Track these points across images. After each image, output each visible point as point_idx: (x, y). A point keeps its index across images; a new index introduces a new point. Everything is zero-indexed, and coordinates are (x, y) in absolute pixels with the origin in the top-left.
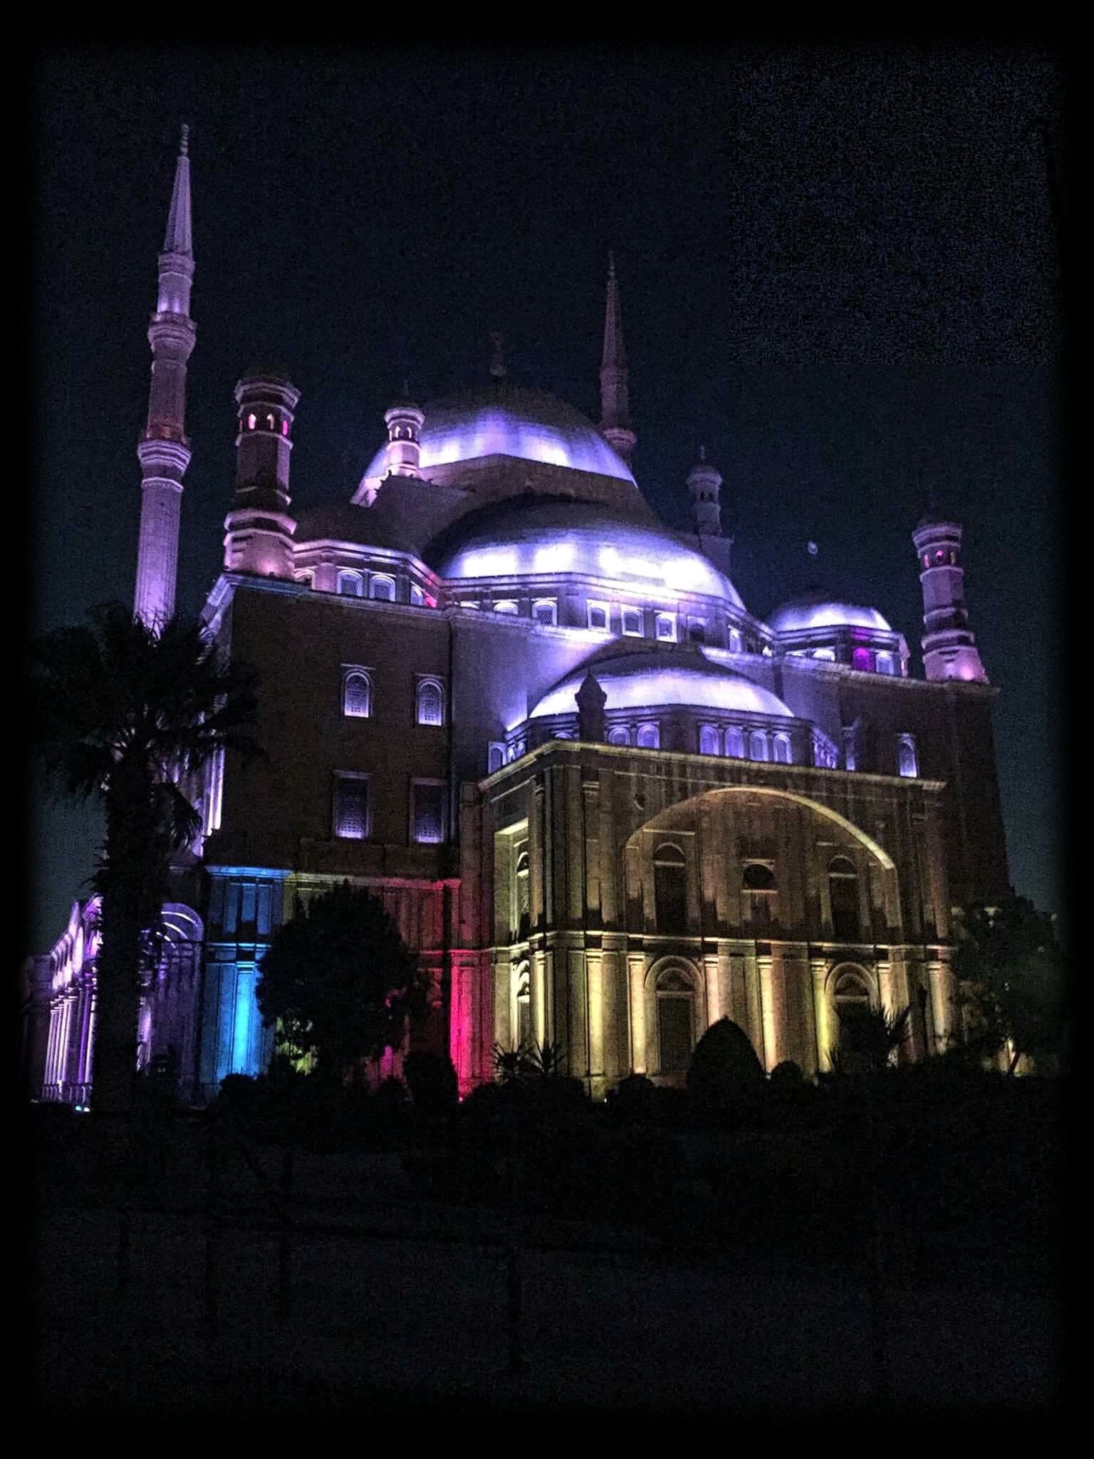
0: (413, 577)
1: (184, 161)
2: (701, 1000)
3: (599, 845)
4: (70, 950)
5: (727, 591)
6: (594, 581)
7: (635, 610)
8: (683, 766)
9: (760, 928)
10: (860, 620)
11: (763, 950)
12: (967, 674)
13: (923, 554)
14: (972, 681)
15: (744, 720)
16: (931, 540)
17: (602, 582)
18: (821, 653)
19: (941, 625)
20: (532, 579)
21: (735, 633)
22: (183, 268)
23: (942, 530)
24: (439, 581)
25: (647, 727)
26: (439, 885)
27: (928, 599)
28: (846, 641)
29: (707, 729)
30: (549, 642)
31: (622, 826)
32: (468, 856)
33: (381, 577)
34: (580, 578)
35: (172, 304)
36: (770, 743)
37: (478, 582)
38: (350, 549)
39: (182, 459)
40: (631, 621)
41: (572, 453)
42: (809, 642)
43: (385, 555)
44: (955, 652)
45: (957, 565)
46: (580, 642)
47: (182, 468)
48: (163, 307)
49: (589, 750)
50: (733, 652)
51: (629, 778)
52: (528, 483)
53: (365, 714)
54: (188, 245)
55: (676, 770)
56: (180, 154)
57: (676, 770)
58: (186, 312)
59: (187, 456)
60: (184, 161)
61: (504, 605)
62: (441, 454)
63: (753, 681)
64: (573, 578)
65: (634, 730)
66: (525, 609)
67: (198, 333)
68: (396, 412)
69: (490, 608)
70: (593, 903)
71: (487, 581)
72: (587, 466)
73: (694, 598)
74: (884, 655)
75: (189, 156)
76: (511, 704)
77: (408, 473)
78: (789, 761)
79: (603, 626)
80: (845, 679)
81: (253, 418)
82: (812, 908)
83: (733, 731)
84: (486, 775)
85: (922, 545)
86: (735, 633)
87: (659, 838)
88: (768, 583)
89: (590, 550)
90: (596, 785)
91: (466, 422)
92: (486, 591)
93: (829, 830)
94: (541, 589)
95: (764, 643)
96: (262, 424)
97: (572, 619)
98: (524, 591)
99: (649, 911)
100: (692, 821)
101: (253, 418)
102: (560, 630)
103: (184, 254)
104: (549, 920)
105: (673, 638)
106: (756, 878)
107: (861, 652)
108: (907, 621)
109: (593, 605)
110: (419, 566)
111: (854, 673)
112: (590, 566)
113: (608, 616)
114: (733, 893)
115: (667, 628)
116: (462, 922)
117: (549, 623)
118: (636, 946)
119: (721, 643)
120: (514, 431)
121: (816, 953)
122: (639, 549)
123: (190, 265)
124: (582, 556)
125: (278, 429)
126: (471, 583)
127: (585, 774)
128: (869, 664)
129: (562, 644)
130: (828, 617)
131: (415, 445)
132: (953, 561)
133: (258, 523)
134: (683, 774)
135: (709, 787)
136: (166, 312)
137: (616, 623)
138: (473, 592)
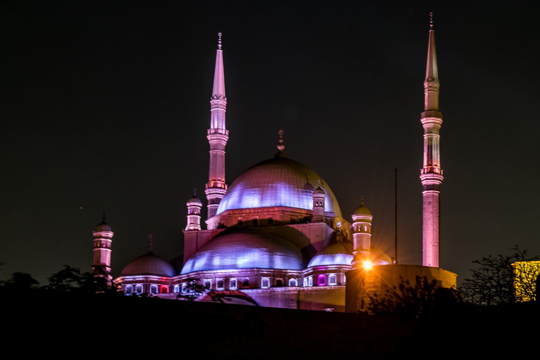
1: (220, 53)
6: (206, 272)
7: (221, 279)
33: (138, 285)
35: (218, 123)
38: (129, 278)
40: (220, 284)
43: (140, 278)
52: (240, 218)
56: (218, 48)
60: (220, 53)
64: (199, 272)
122: (228, 255)
123: (223, 102)
128: (324, 281)
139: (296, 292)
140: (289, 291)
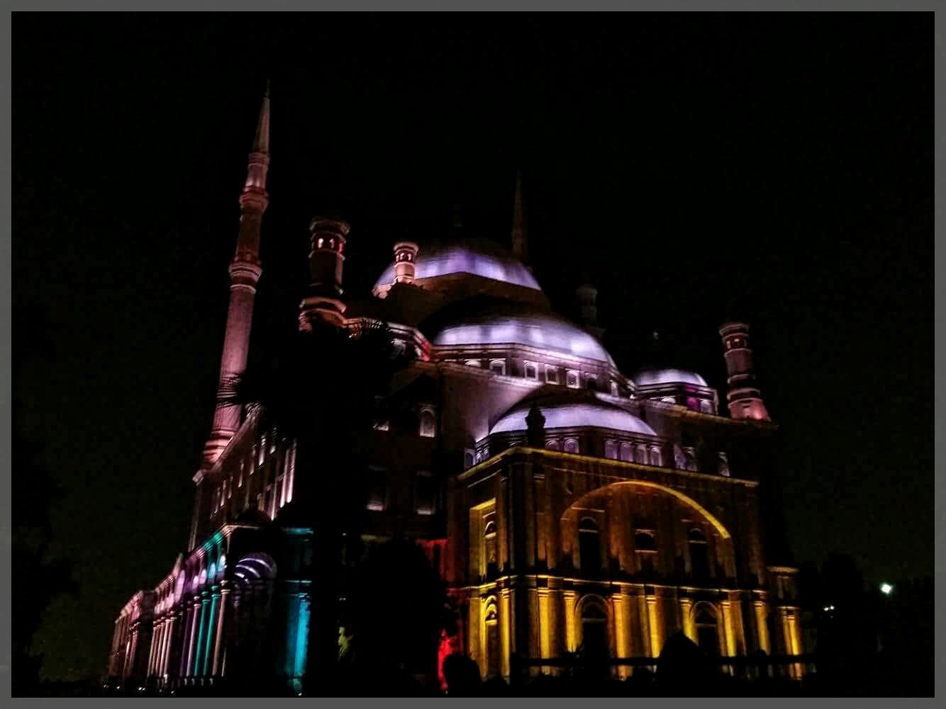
0: (417, 343)
1: (267, 103)
2: (610, 626)
3: (544, 516)
4: (172, 587)
5: (608, 359)
6: (528, 349)
8: (596, 465)
9: (645, 575)
10: (690, 380)
11: (650, 591)
12: (758, 415)
13: (727, 340)
14: (762, 421)
15: (632, 437)
16: (730, 332)
17: (533, 350)
18: (666, 399)
19: (739, 384)
20: (490, 347)
21: (614, 385)
22: (263, 162)
23: (738, 326)
24: (431, 347)
25: (571, 441)
26: (432, 543)
27: (730, 369)
28: (681, 392)
29: (609, 442)
30: (501, 386)
31: (559, 505)
32: (451, 526)
34: (520, 347)
36: (649, 452)
37: (455, 348)
39: (256, 273)
40: (551, 375)
41: (507, 273)
42: (659, 392)
44: (749, 401)
45: (747, 347)
46: (525, 385)
47: (256, 278)
48: (250, 183)
49: (539, 454)
50: (614, 396)
51: (563, 472)
53: (387, 429)
54: (267, 149)
55: (591, 468)
56: (265, 96)
57: (591, 468)
58: (264, 187)
59: (259, 271)
60: (267, 103)
61: (473, 362)
62: (428, 271)
63: (633, 414)
64: (516, 346)
65: (562, 442)
66: (485, 365)
67: (269, 199)
68: (401, 245)
69: (464, 363)
70: (542, 555)
71: (461, 347)
72: (515, 281)
73: (589, 361)
74: (705, 402)
75: (270, 98)
76: (478, 424)
77: (409, 281)
78: (660, 465)
79: (534, 377)
80: (684, 416)
81: (321, 241)
82: (680, 562)
83: (626, 445)
84: (463, 471)
85: (725, 334)
86: (614, 385)
87: (580, 514)
88: (631, 354)
89: (525, 330)
90: (542, 477)
91: (442, 252)
92: (460, 353)
93: (688, 512)
94: (496, 353)
95: (631, 392)
96: (326, 244)
97: (515, 371)
98: (485, 354)
99: (576, 563)
100: (602, 502)
101: (321, 241)
102: (509, 378)
103: (264, 153)
104: (512, 567)
105: (577, 386)
106: (644, 542)
107: (692, 400)
108: (716, 379)
109: (527, 363)
110: (419, 336)
111: (689, 412)
112: (526, 339)
113: (537, 371)
114: (629, 551)
115: (573, 380)
116: (447, 568)
117: (501, 374)
118: (569, 586)
119: (607, 390)
120: (472, 260)
121: (684, 594)
123: (267, 159)
124: (520, 333)
125: (337, 248)
126: (451, 348)
127: (537, 469)
129: (509, 388)
130: (669, 377)
131: (411, 264)
132: (745, 345)
133: (323, 305)
134: (596, 471)
135: (613, 481)
136: (251, 186)
137: (542, 376)
138: (452, 354)
139: (679, 416)
140: (672, 411)
